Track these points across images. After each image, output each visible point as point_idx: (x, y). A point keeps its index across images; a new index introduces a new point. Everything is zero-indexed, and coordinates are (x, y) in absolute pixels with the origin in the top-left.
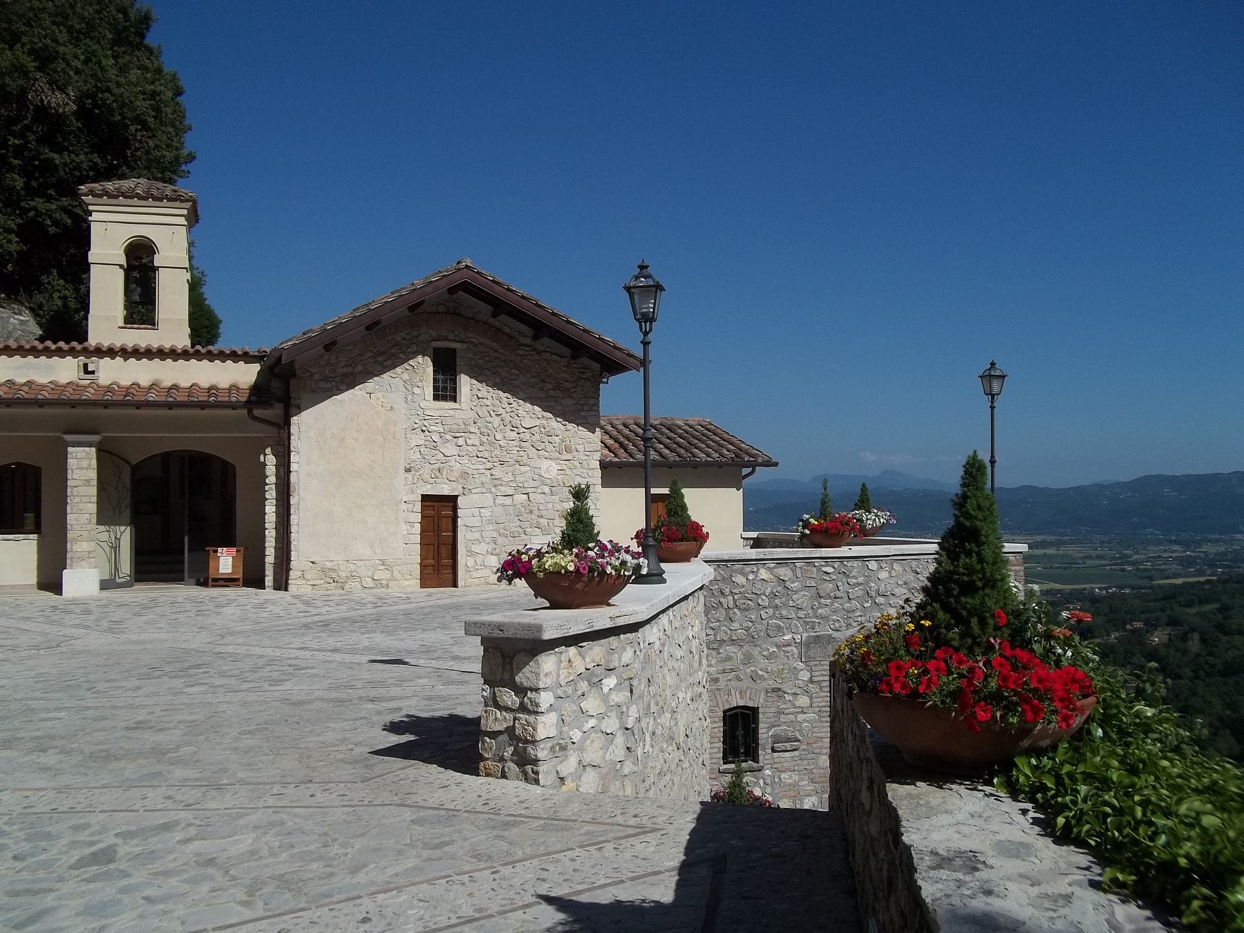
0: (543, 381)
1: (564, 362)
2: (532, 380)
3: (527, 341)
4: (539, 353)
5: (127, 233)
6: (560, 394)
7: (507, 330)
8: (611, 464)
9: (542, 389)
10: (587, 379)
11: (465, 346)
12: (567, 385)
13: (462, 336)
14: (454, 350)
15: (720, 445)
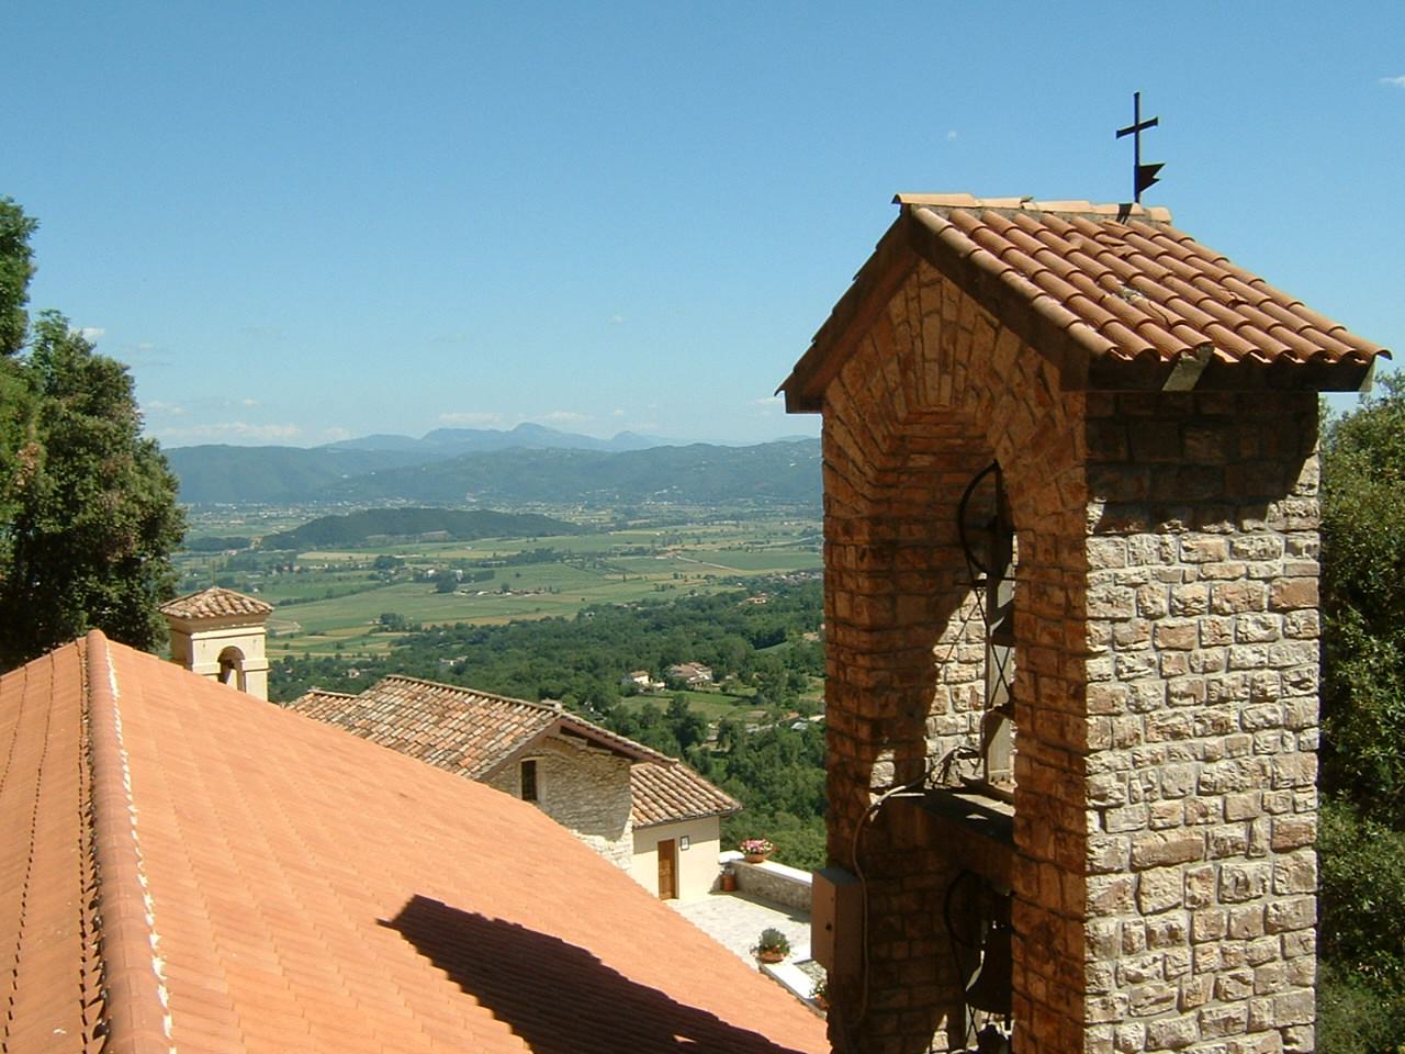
0: (594, 775)
1: (608, 758)
2: (588, 776)
3: (584, 747)
4: (591, 755)
5: (221, 646)
6: (605, 782)
7: (570, 742)
8: (639, 827)
9: (593, 781)
10: (623, 769)
11: (543, 758)
12: (610, 775)
13: (541, 751)
14: (533, 763)
15: (701, 793)
